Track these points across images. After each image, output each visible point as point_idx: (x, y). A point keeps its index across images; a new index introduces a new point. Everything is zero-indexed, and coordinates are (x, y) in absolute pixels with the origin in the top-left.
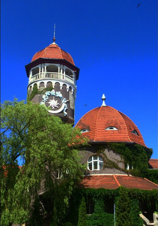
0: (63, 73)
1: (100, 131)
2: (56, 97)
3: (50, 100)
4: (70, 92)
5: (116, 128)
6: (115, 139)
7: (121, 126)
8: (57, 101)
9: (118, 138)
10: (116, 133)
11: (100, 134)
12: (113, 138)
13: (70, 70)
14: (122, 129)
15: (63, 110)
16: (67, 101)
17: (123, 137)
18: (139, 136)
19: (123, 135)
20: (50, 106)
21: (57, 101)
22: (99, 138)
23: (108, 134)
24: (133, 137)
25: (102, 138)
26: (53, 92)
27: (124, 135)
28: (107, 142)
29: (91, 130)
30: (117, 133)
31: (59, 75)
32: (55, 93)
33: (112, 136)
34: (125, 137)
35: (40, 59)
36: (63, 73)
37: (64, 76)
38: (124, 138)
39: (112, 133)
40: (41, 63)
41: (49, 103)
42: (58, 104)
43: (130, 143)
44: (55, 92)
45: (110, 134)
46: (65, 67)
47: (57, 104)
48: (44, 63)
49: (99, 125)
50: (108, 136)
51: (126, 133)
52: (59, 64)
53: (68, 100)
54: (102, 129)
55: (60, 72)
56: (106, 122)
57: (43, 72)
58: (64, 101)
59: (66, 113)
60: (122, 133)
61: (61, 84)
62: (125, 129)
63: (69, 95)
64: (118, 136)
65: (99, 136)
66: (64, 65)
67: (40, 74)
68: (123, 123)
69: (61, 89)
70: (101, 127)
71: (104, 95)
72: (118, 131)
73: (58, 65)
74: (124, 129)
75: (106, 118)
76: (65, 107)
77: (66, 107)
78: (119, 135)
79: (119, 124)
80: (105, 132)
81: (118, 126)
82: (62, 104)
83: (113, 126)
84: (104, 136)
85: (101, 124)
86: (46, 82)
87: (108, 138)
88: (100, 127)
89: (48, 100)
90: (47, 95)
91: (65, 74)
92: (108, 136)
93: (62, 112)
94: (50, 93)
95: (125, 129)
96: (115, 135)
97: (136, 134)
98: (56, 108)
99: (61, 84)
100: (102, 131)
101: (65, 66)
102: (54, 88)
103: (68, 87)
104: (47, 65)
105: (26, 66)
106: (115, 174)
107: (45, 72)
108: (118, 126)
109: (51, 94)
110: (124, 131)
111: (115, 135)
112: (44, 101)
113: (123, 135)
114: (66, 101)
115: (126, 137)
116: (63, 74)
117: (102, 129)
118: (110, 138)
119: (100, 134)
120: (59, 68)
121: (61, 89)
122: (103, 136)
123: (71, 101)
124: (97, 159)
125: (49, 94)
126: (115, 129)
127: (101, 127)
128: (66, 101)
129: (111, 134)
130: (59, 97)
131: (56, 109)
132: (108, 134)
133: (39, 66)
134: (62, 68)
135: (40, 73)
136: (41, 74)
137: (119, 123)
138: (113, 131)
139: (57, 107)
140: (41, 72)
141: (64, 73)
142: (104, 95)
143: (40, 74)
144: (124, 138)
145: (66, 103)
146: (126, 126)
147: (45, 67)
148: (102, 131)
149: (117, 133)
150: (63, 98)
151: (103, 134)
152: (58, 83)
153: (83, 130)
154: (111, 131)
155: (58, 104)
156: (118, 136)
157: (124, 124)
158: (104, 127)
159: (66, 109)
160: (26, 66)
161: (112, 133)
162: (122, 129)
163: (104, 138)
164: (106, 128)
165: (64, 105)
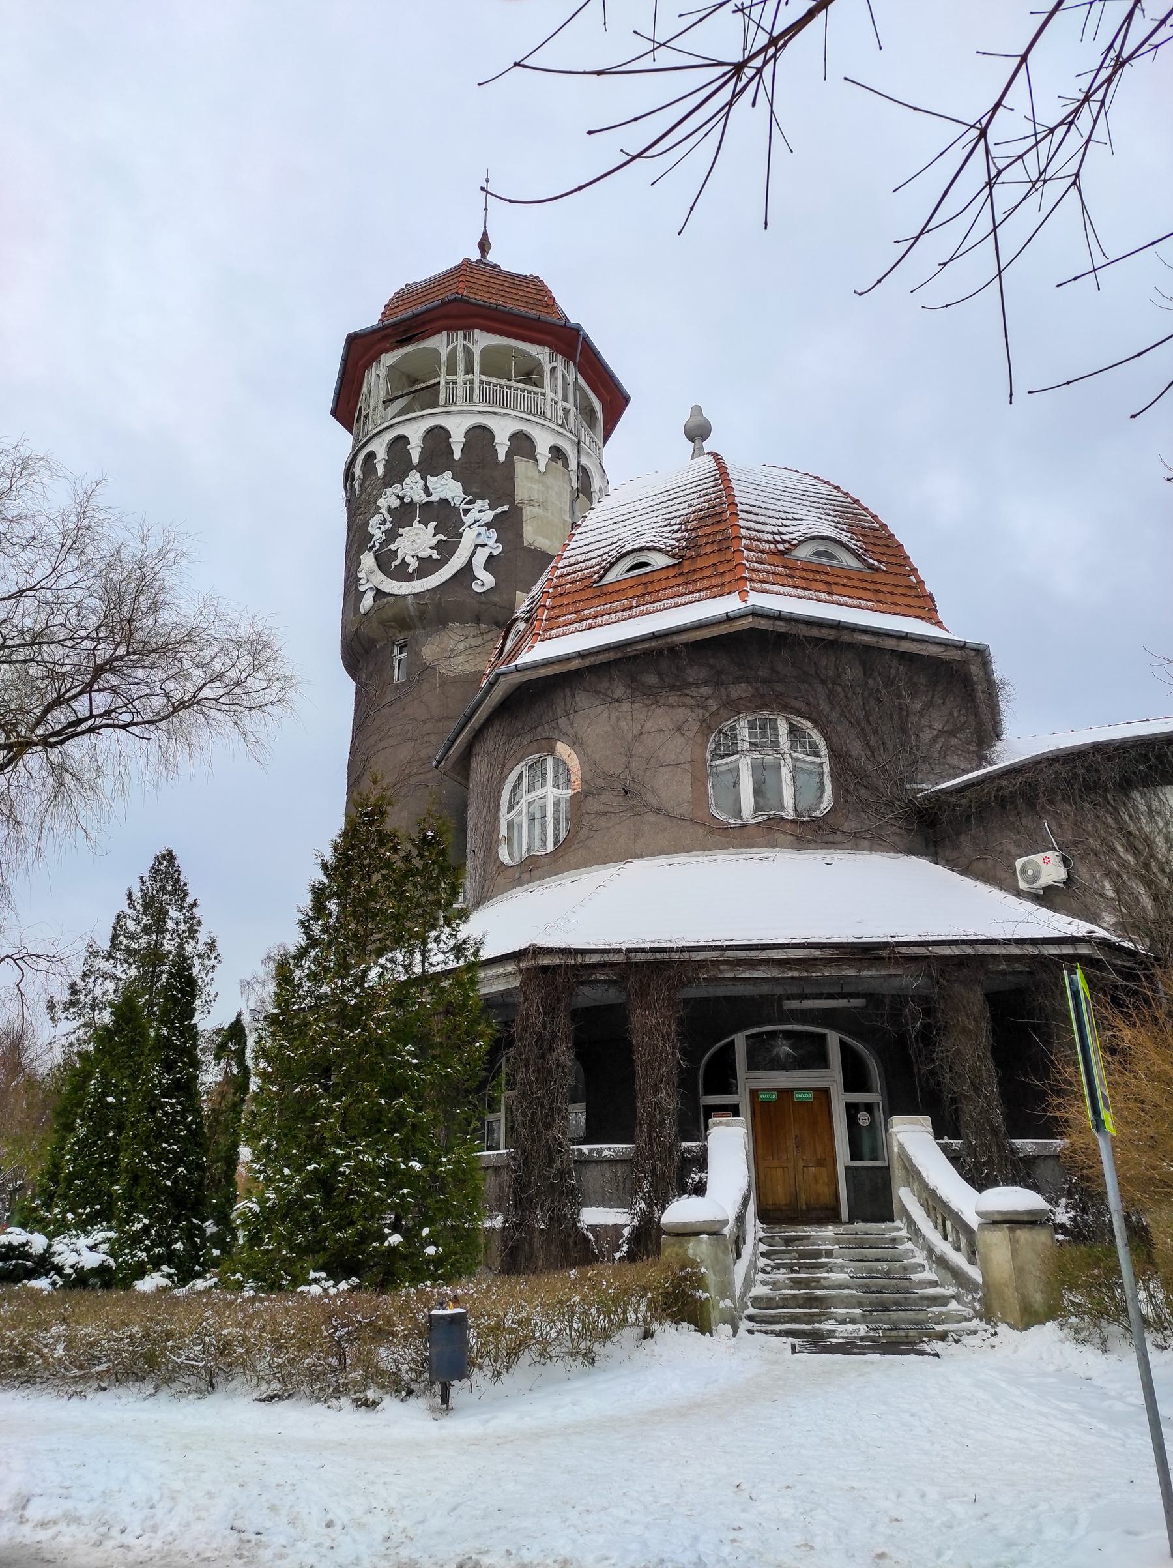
0: (469, 370)
4: (521, 464)
8: (432, 525)
10: (664, 584)
13: (518, 350)
15: (469, 565)
16: (499, 510)
20: (398, 562)
21: (432, 525)
26: (413, 487)
31: (442, 384)
35: (353, 340)
36: (469, 370)
37: (476, 385)
40: (368, 366)
41: (392, 547)
42: (441, 537)
46: (484, 340)
47: (434, 541)
48: (376, 357)
52: (445, 333)
53: (505, 508)
58: (481, 512)
59: (485, 580)
61: (458, 428)
63: (511, 478)
66: (469, 328)
69: (457, 455)
72: (676, 571)
73: (440, 343)
77: (491, 542)
82: (461, 535)
83: (642, 549)
89: (392, 535)
93: (467, 571)
94: (398, 496)
99: (458, 428)
101: (477, 332)
102: (415, 459)
104: (390, 362)
109: (402, 498)
110: (713, 559)
112: (374, 546)
114: (493, 513)
116: (469, 377)
120: (444, 353)
121: (457, 455)
123: (528, 512)
125: (396, 503)
128: (489, 516)
130: (444, 502)
131: (427, 566)
138: (644, 580)
139: (435, 556)
141: (477, 369)
145: (489, 525)
147: (383, 372)
149: (672, 582)
150: (469, 502)
152: (442, 428)
155: (441, 537)
162: (709, 549)
165: (469, 538)
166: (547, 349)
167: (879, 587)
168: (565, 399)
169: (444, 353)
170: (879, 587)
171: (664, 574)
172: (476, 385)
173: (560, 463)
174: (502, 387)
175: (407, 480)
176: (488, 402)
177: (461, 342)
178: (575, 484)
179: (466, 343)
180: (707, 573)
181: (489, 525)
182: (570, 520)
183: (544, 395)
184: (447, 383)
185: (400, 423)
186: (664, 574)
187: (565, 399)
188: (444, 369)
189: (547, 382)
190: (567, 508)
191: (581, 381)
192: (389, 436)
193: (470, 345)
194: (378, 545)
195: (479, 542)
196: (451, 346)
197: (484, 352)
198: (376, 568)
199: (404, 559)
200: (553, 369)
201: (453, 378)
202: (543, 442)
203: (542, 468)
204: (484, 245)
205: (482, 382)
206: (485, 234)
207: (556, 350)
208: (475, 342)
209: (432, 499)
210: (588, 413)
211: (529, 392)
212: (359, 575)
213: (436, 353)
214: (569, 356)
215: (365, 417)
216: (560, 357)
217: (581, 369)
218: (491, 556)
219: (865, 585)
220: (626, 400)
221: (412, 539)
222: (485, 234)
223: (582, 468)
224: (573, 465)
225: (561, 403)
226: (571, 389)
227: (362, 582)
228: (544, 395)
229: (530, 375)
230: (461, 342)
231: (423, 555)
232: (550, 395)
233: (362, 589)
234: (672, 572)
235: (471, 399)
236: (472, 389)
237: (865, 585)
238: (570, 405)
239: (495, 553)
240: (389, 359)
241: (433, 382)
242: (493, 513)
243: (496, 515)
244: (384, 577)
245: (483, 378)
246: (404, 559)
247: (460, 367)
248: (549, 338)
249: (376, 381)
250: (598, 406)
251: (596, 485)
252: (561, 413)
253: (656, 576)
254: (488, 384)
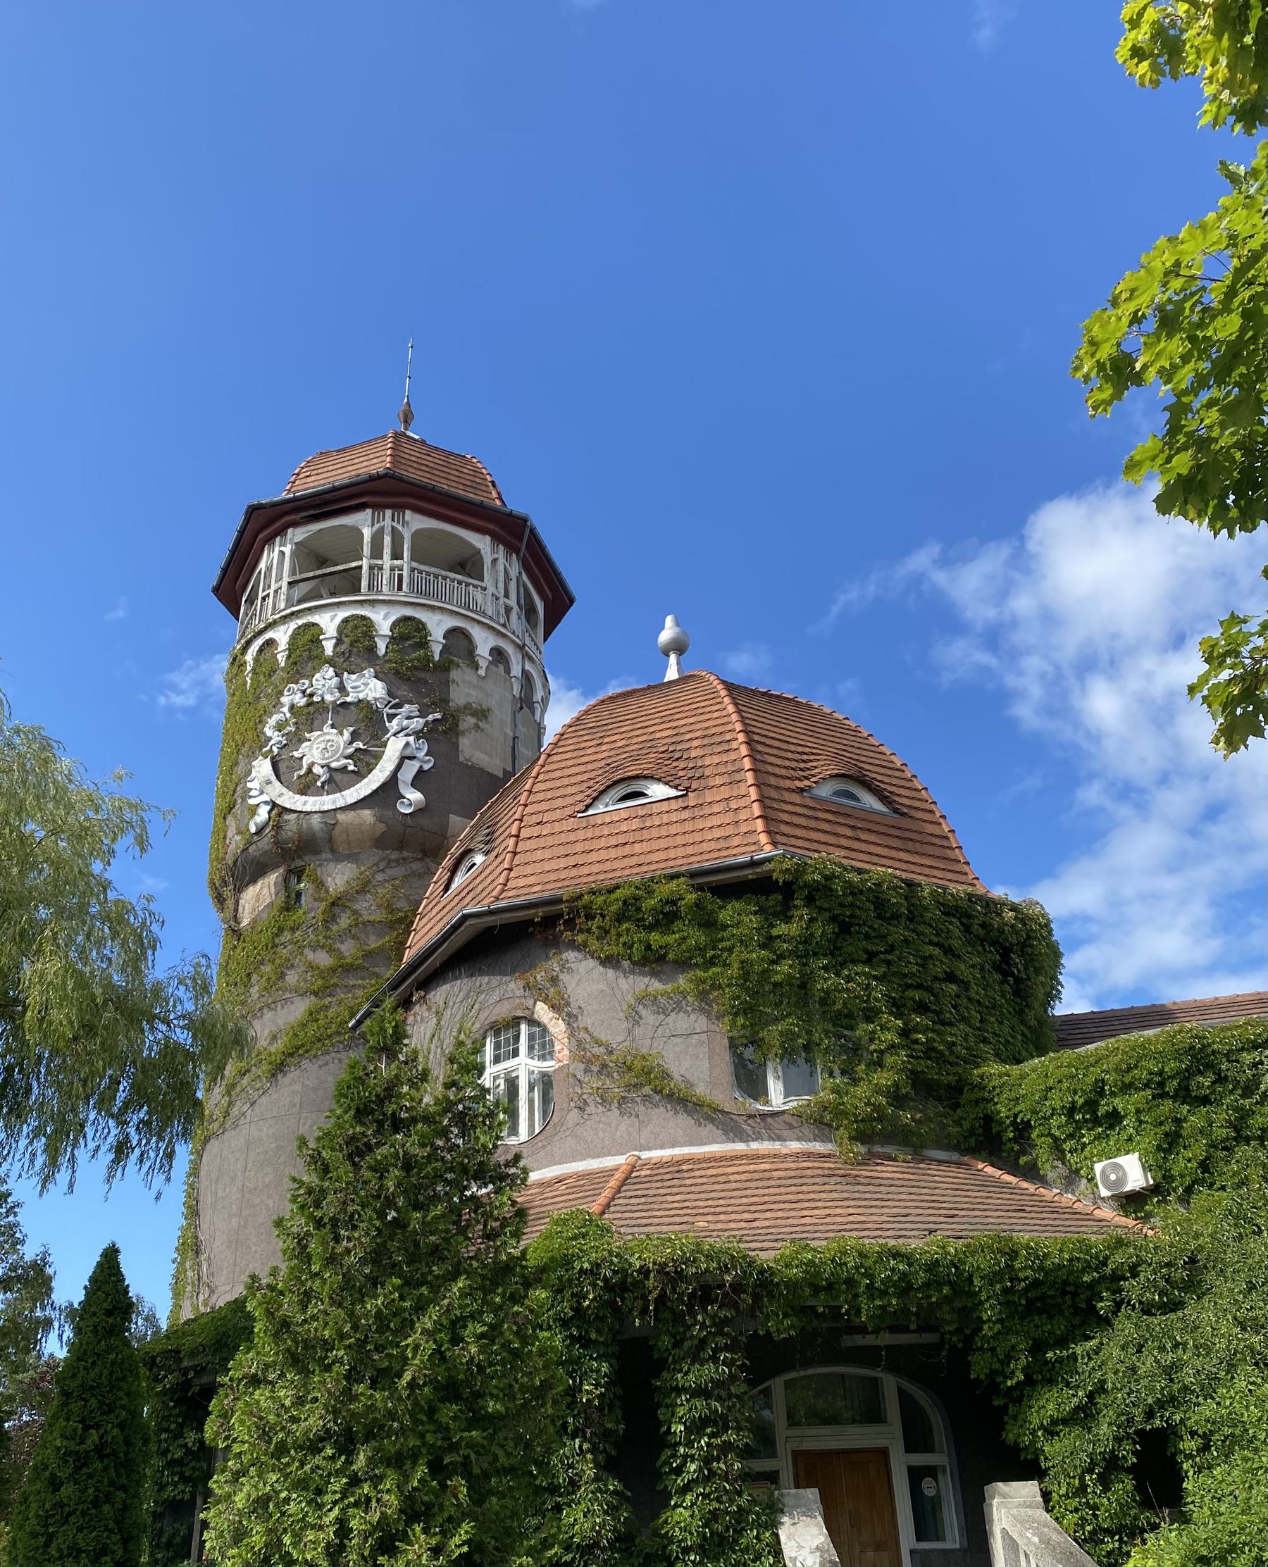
0: (397, 555)
1: (546, 830)
2: (344, 704)
3: (307, 735)
5: (667, 783)
6: (644, 869)
7: (707, 761)
9: (672, 853)
10: (665, 819)
11: (538, 855)
12: (634, 861)
14: (718, 780)
16: (430, 717)
17: (717, 833)
18: (904, 822)
19: (716, 821)
20: (303, 772)
22: (531, 880)
23: (603, 843)
24: (827, 827)
25: (553, 876)
27: (728, 818)
28: (557, 901)
29: (498, 842)
30: (674, 817)
32: (342, 688)
33: (627, 850)
34: (730, 830)
35: (253, 510)
37: (405, 573)
38: (722, 844)
39: (635, 824)
40: (270, 540)
41: (296, 754)
43: (753, 864)
44: (336, 680)
45: (613, 841)
46: (416, 522)
47: (351, 750)
48: (282, 531)
49: (540, 796)
50: (603, 855)
51: (742, 803)
52: (369, 511)
53: (438, 716)
54: (558, 814)
55: (377, 553)
56: (603, 763)
59: (415, 796)
60: (707, 811)
61: (383, 621)
62: (737, 777)
64: (679, 840)
65: (528, 870)
66: (399, 508)
67: (264, 599)
68: (728, 737)
70: (560, 802)
71: (669, 621)
72: (680, 803)
73: (364, 523)
74: (725, 779)
75: (606, 740)
76: (403, 759)
77: (421, 754)
78: (688, 826)
79: (694, 754)
80: (581, 835)
81: (682, 765)
83: (637, 777)
84: (572, 861)
85: (558, 783)
86: (282, 636)
87: (595, 868)
88: (545, 806)
89: (296, 739)
90: (285, 709)
91: (413, 558)
92: (603, 855)
93: (390, 788)
95: (737, 777)
96: (655, 833)
97: (870, 801)
98: (338, 777)
99: (383, 621)
100: (557, 827)
101: (408, 513)
103: (437, 626)
104: (298, 539)
105: (216, 590)
106: (645, 1155)
108: (682, 765)
110: (725, 792)
111: (655, 833)
113: (716, 821)
115: (744, 828)
117: (558, 814)
118: (608, 866)
119: (538, 855)
120: (367, 533)
122: (563, 863)
124: (516, 1053)
125: (300, 701)
126: (658, 791)
127: (560, 802)
128: (417, 723)
129: (622, 839)
131: (336, 780)
132: (603, 843)
134: (388, 530)
136: (268, 595)
137: (695, 743)
138: (641, 813)
139: (351, 768)
142: (669, 621)
144: (722, 844)
145: (418, 734)
146: (744, 750)
148: (557, 827)
149: (674, 817)
151: (562, 850)
153: (463, 868)
154: (624, 815)
156: (679, 840)
157: (734, 745)
158: (580, 797)
159: (410, 770)
160: (216, 590)
161: (635, 824)
162: (718, 780)
163: (563, 875)
164: (589, 801)
166: (488, 538)
167: (907, 834)
168: (507, 595)
169: (367, 533)
170: (907, 834)
171: (664, 807)
172: (405, 573)
173: (501, 667)
174: (436, 577)
175: (317, 676)
176: (420, 593)
177: (388, 522)
178: (516, 691)
179: (395, 524)
180: (716, 808)
181: (418, 734)
182: (511, 734)
183: (485, 589)
184: (371, 568)
185: (309, 609)
186: (664, 807)
187: (507, 595)
188: (366, 550)
189: (486, 576)
190: (509, 720)
191: (524, 577)
192: (293, 625)
193: (400, 528)
194: (275, 750)
195: (408, 753)
196: (377, 526)
197: (416, 535)
198: (273, 778)
199: (310, 771)
200: (495, 561)
201: (380, 562)
202: (484, 643)
203: (482, 672)
204: (407, 419)
205: (413, 570)
207: (497, 539)
208: (405, 524)
209: (348, 699)
210: (530, 611)
211: (467, 585)
212: (249, 785)
214: (511, 548)
215: (264, 599)
216: (501, 548)
217: (526, 566)
218: (420, 771)
219: (893, 832)
220: (572, 601)
221: (323, 746)
223: (526, 675)
224: (516, 670)
225: (502, 600)
226: (513, 585)
227: (252, 793)
228: (485, 589)
229: (468, 565)
230: (388, 522)
231: (334, 765)
232: (491, 589)
233: (252, 802)
234: (674, 805)
235: (400, 588)
236: (400, 577)
237: (893, 832)
238: (512, 602)
239: (426, 767)
240: (298, 534)
241: (354, 564)
242: (422, 721)
243: (427, 723)
244: (285, 790)
245: (415, 565)
246: (310, 771)
247: (387, 551)
248: (492, 526)
249: (277, 560)
251: (539, 694)
252: (502, 611)
253: (656, 808)
254: (420, 572)
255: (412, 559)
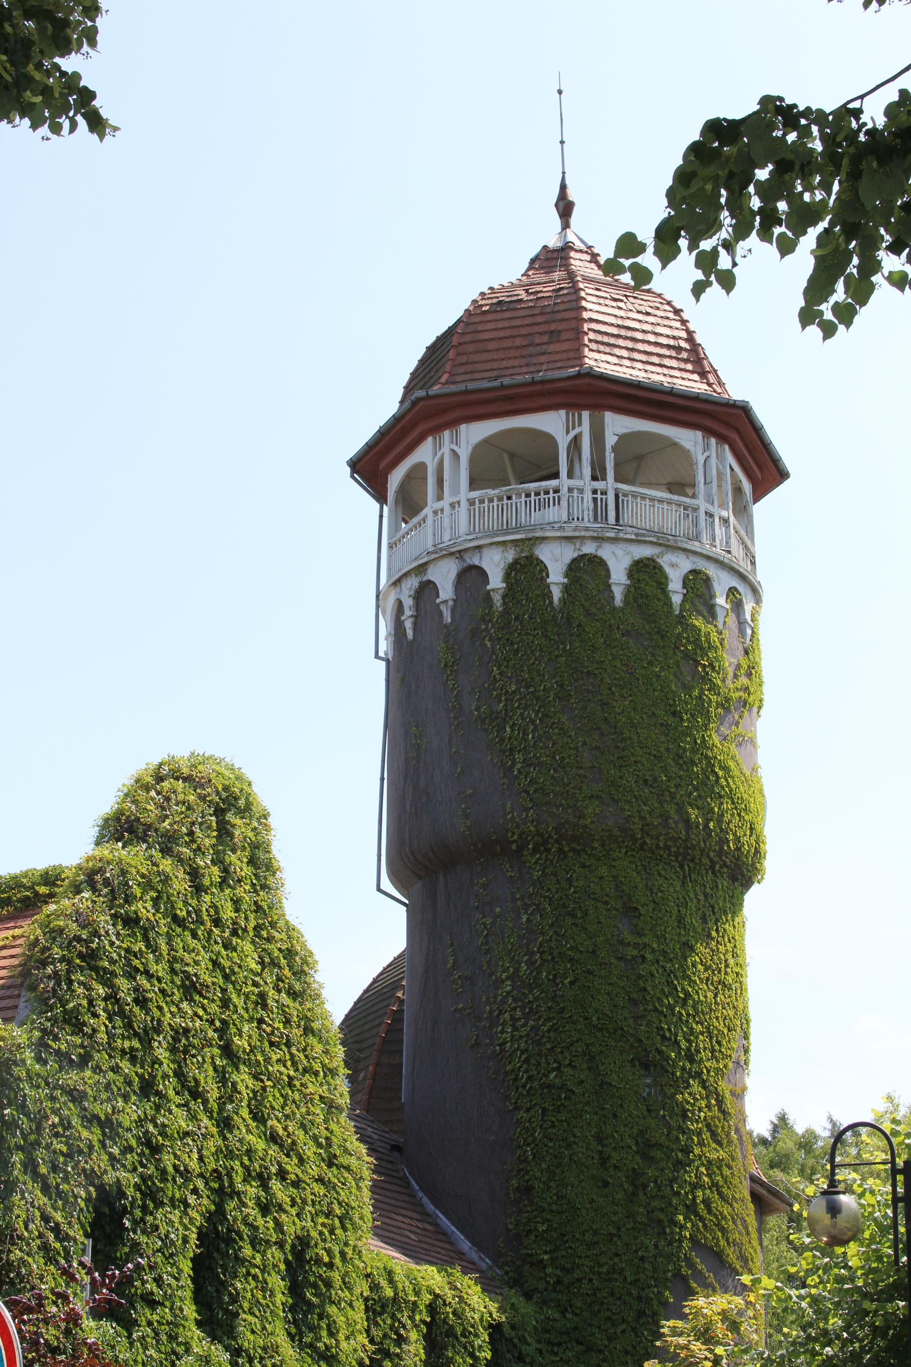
40: (436, 430)
46: (617, 425)
48: (453, 424)
52: (563, 413)
57: (448, 498)
107: (465, 493)
120: (563, 442)
133: (424, 453)
135: (432, 504)
140: (440, 497)
143: (435, 513)
147: (464, 454)
166: (699, 434)
169: (563, 442)
184: (570, 490)
196: (572, 434)
206: (563, 187)
207: (708, 432)
213: (549, 441)
216: (713, 441)
222: (563, 187)
240: (475, 433)
250: (747, 486)
255: (617, 480)
